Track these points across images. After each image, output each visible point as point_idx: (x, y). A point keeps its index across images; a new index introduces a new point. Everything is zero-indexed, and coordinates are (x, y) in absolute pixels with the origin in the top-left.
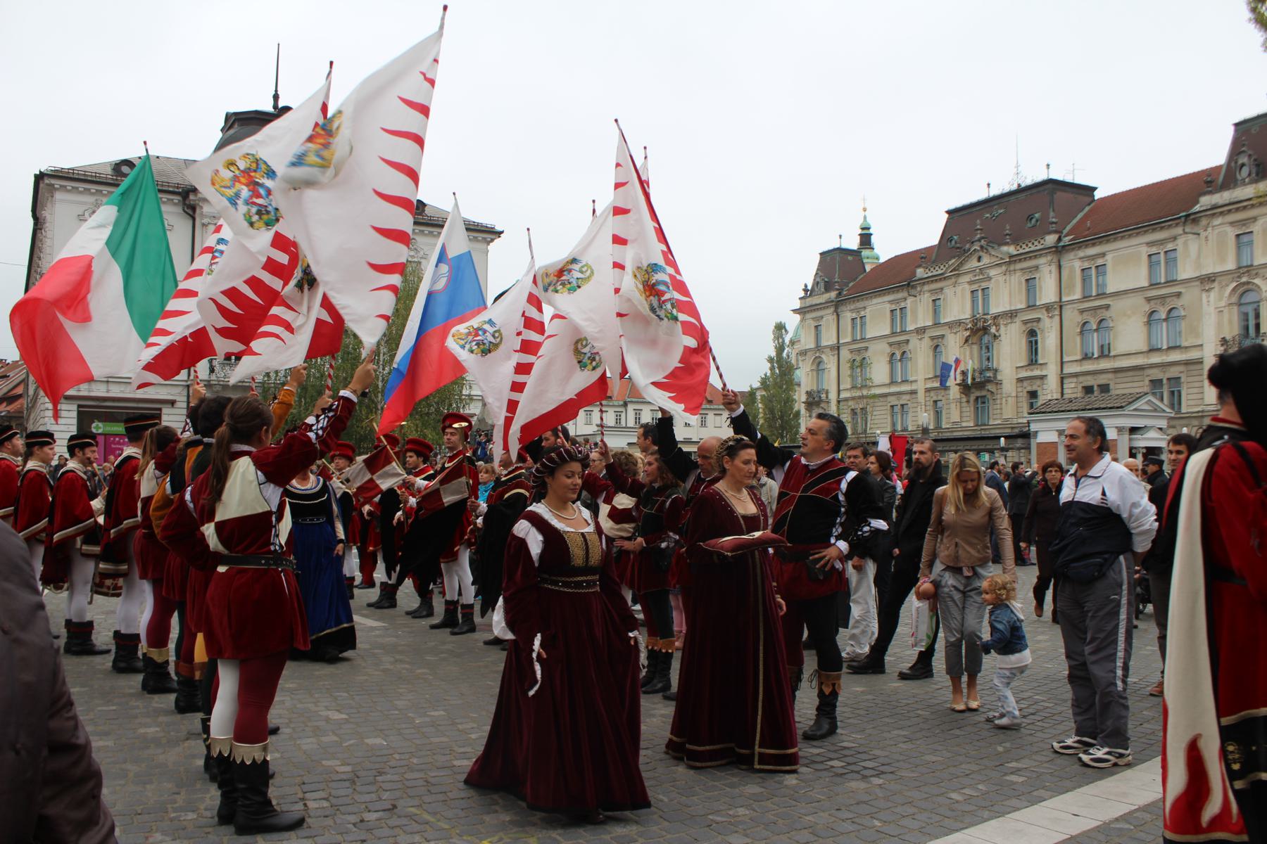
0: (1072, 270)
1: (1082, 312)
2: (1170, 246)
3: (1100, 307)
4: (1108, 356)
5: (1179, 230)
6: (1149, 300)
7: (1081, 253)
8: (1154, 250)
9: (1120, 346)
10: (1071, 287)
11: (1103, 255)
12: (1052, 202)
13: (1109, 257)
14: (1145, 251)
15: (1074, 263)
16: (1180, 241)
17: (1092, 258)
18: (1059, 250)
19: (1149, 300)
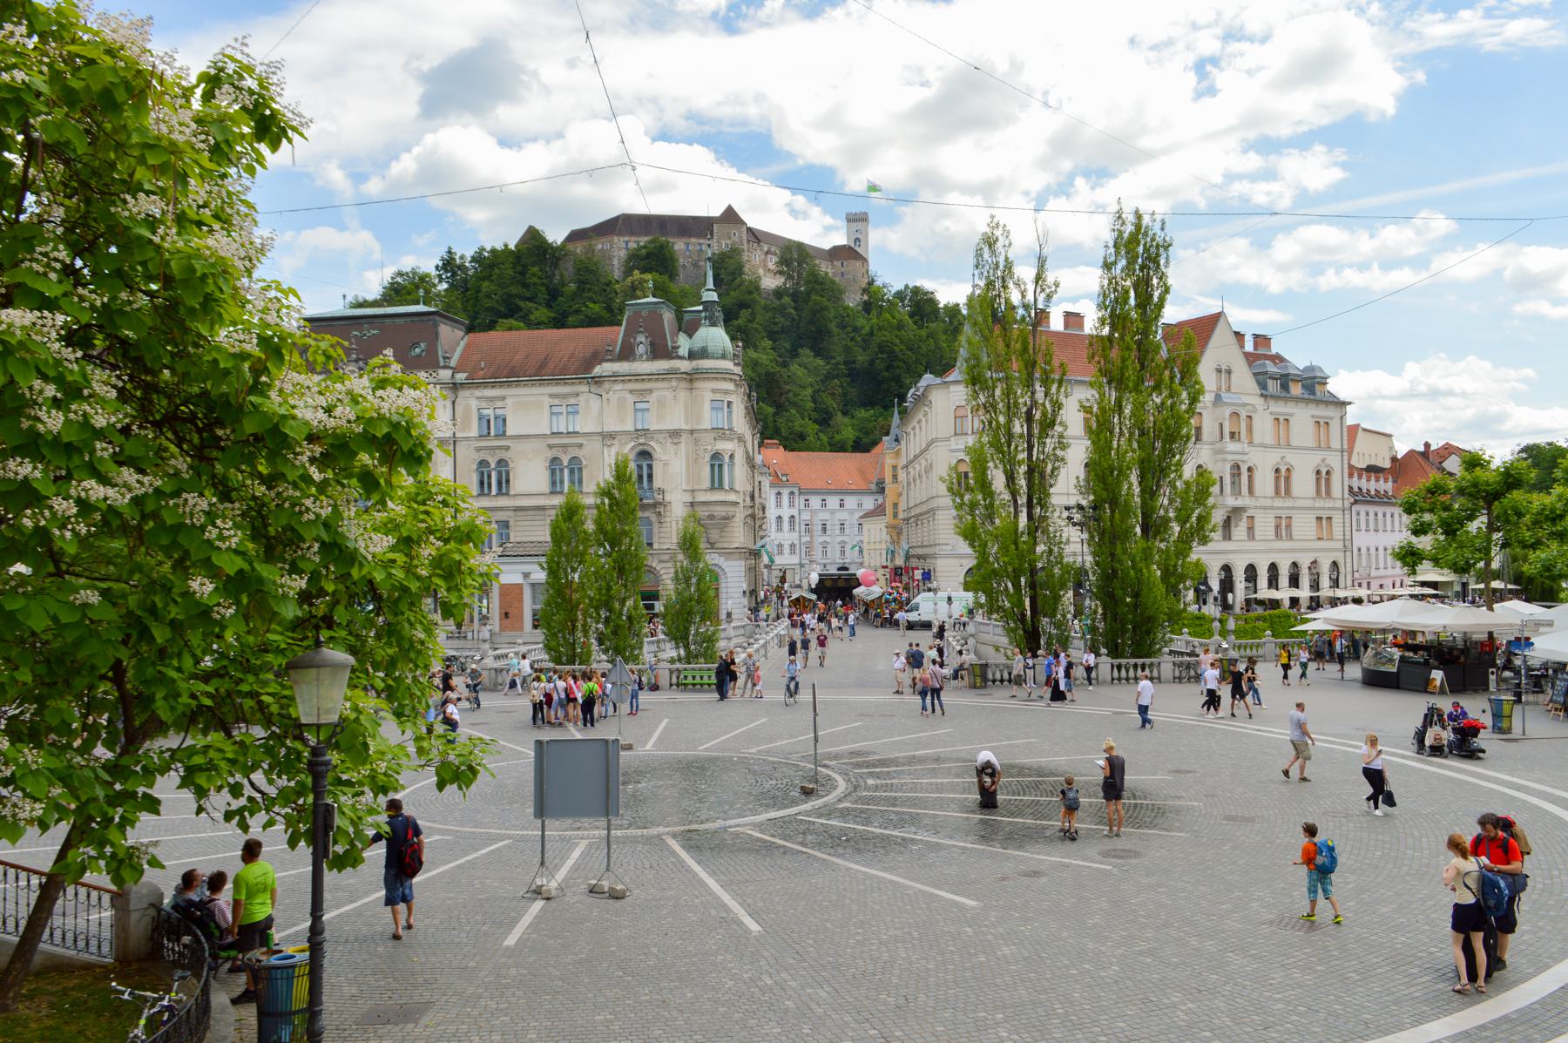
0: (467, 408)
1: (478, 450)
2: (572, 401)
3: (499, 448)
4: (507, 494)
5: (584, 388)
6: (550, 447)
7: (478, 393)
8: (557, 402)
9: (517, 485)
10: (466, 425)
11: (504, 398)
12: (437, 334)
13: (509, 401)
14: (547, 401)
15: (471, 401)
16: (582, 398)
17: (491, 399)
18: (455, 387)
19: (550, 447)
